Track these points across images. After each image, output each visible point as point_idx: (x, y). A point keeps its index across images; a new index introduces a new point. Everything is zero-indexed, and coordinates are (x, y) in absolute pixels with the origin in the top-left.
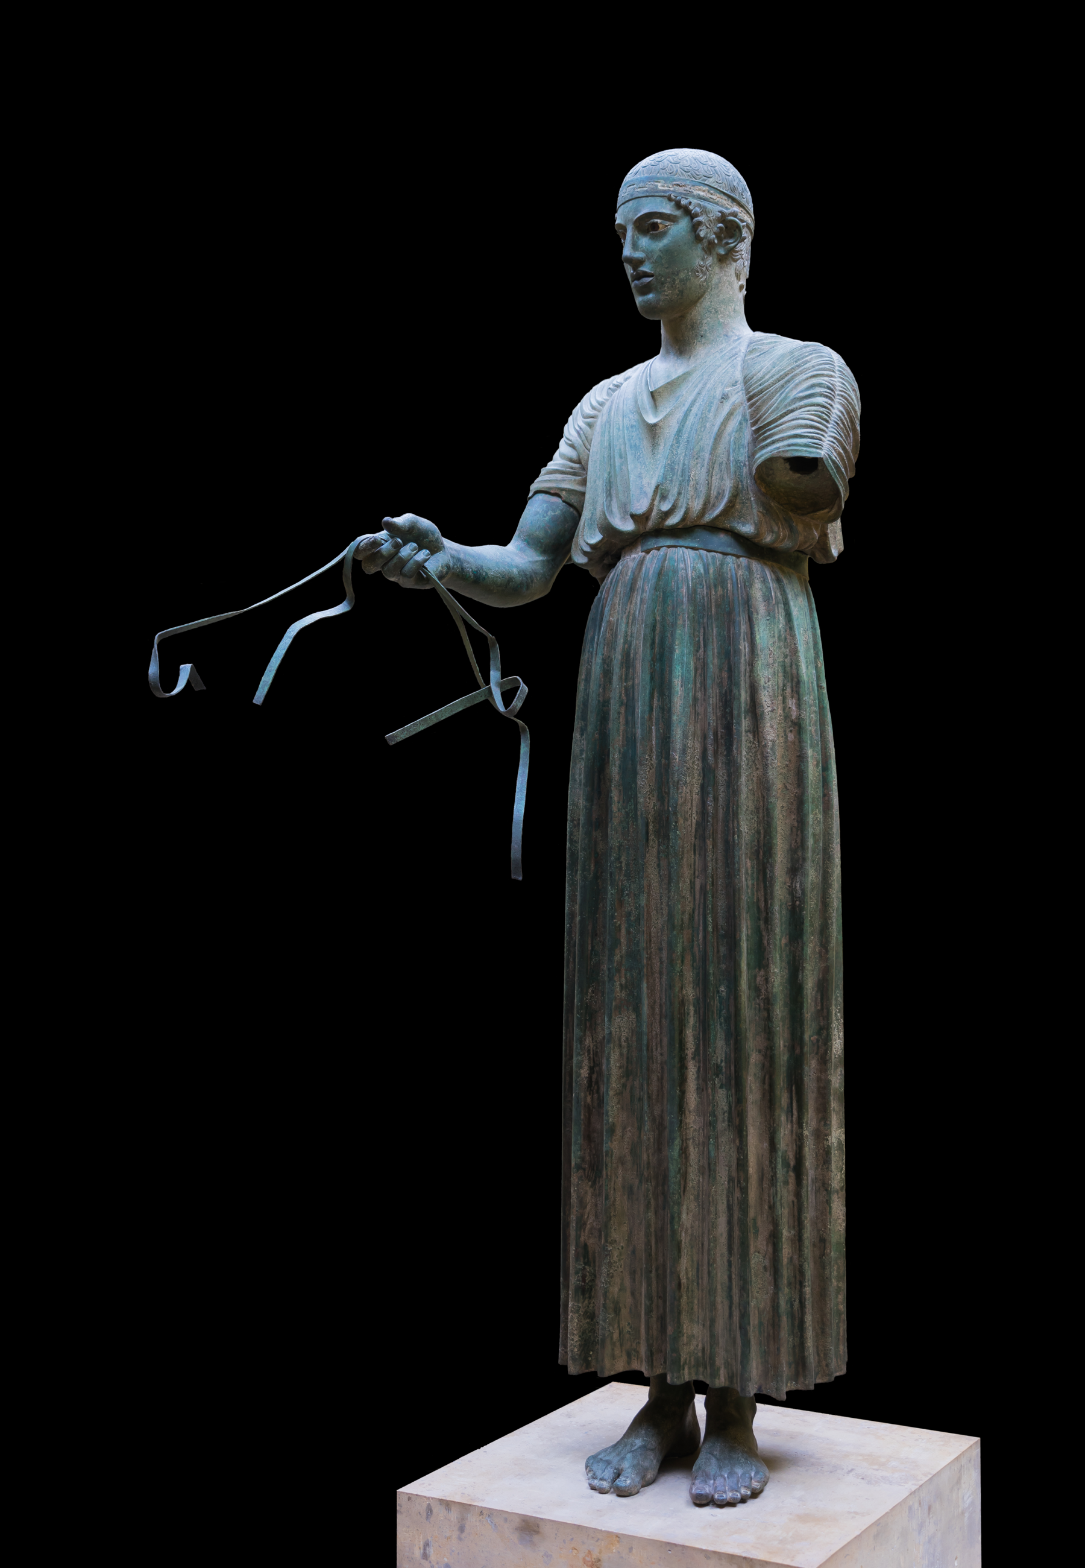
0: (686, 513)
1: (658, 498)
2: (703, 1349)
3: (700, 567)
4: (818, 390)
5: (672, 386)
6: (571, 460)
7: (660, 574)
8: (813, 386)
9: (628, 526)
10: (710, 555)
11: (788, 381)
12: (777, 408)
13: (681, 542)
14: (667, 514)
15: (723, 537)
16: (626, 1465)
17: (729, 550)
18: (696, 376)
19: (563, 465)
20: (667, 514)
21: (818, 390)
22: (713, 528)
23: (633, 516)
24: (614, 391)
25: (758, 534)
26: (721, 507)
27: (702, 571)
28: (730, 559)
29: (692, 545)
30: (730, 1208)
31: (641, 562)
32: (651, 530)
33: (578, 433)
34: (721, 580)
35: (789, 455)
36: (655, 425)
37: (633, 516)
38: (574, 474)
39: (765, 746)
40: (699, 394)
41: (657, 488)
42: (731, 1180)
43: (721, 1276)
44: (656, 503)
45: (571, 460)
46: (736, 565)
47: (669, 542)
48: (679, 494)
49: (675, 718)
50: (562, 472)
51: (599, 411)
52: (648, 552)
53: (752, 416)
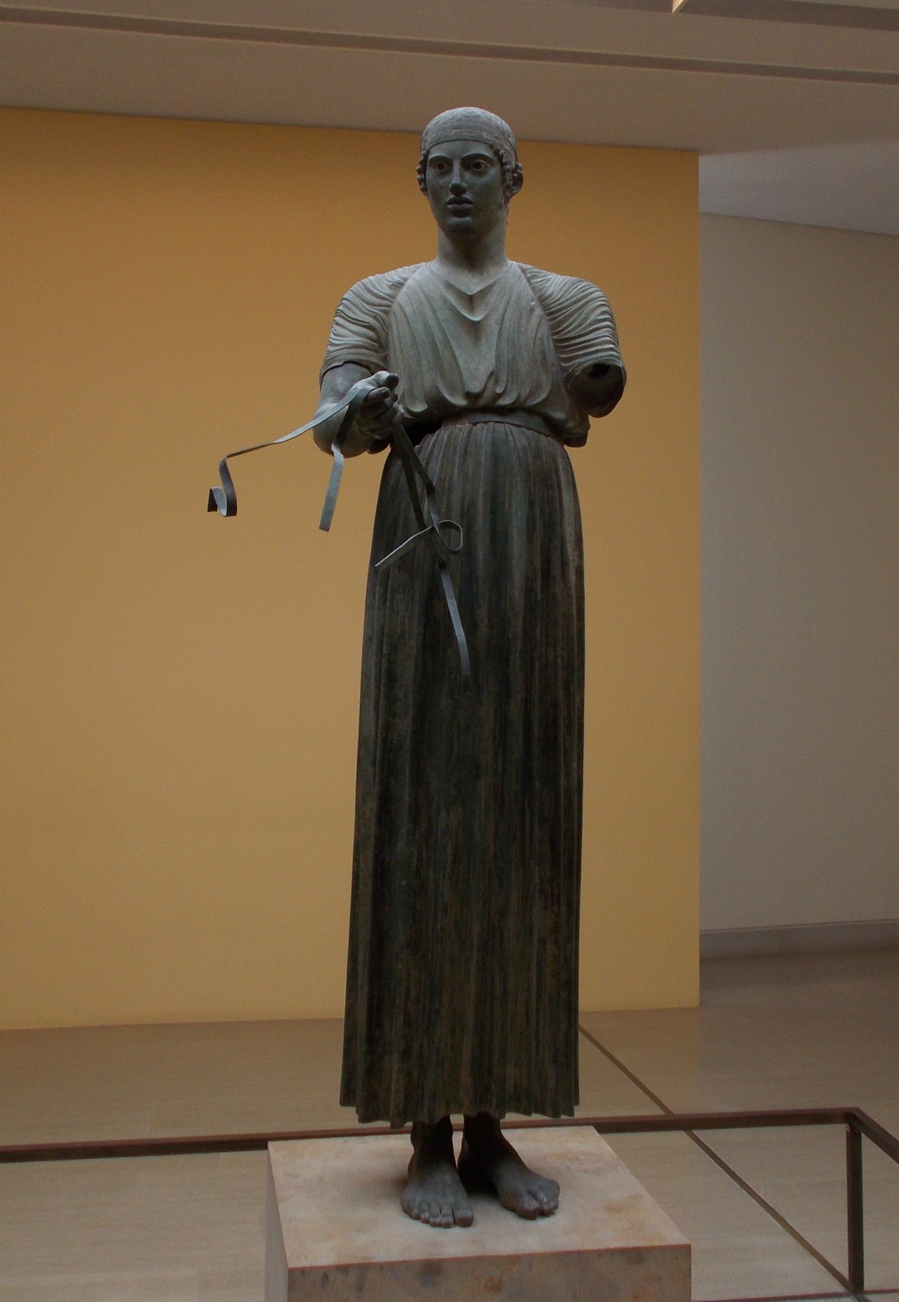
0: (519, 397)
1: (492, 382)
2: (515, 1086)
3: (524, 440)
4: (607, 316)
5: (484, 293)
6: (371, 339)
7: (494, 443)
8: (603, 313)
9: (459, 401)
10: (529, 433)
11: (583, 305)
12: (580, 325)
13: (507, 420)
14: (499, 396)
15: (536, 421)
16: (451, 1199)
17: (542, 430)
18: (496, 289)
19: (366, 343)
20: (499, 396)
21: (607, 316)
22: (531, 411)
23: (468, 395)
24: (400, 288)
25: (566, 421)
26: (543, 396)
27: (526, 444)
28: (543, 437)
29: (516, 423)
30: (539, 964)
31: (470, 432)
32: (480, 407)
33: (375, 318)
34: (538, 454)
35: (610, 363)
36: (478, 322)
37: (468, 395)
38: (376, 351)
39: (570, 588)
40: (508, 303)
41: (492, 373)
42: (543, 941)
43: (534, 1024)
44: (491, 385)
45: (371, 339)
46: (547, 442)
47: (496, 419)
48: (508, 381)
49: (514, 562)
50: (366, 348)
51: (392, 302)
52: (475, 424)
53: (554, 327)
